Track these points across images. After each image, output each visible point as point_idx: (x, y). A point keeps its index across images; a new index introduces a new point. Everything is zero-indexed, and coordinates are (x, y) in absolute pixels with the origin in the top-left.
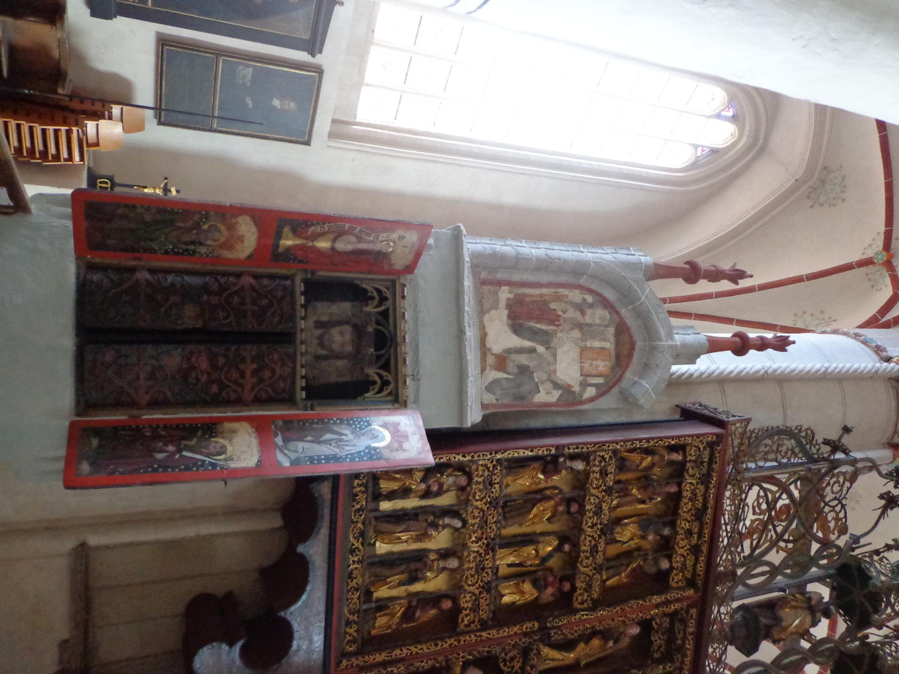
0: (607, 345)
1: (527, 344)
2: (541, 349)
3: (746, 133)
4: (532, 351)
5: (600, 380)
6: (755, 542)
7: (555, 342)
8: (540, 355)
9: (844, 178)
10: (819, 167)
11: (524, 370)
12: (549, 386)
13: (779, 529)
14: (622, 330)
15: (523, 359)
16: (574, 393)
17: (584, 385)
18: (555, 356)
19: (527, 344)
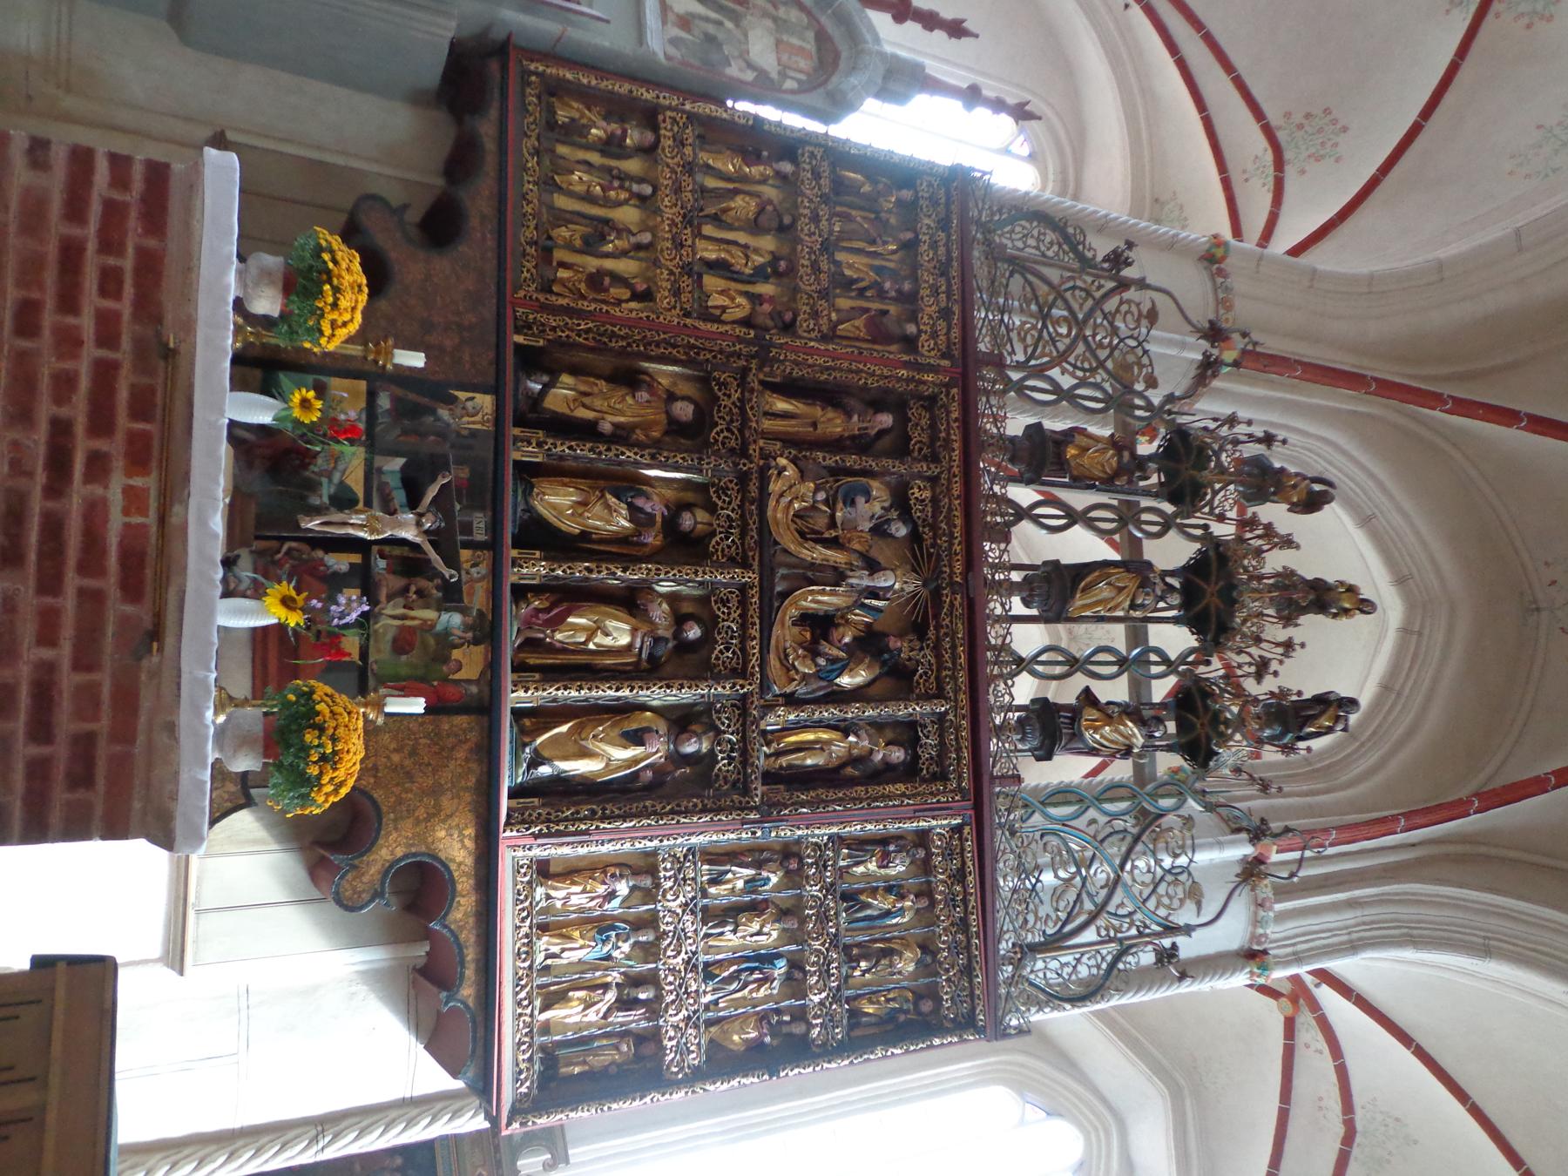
0: (808, 47)
1: (713, 15)
2: (729, 24)
3: (1051, 177)
4: (720, 23)
5: (803, 77)
6: (1030, 350)
7: (745, 23)
8: (729, 31)
9: (1181, 207)
10: (1148, 201)
11: (710, 39)
12: (743, 65)
13: (1061, 347)
14: (822, 37)
15: (711, 29)
16: (772, 81)
17: (783, 75)
18: (746, 36)
19: (713, 15)
